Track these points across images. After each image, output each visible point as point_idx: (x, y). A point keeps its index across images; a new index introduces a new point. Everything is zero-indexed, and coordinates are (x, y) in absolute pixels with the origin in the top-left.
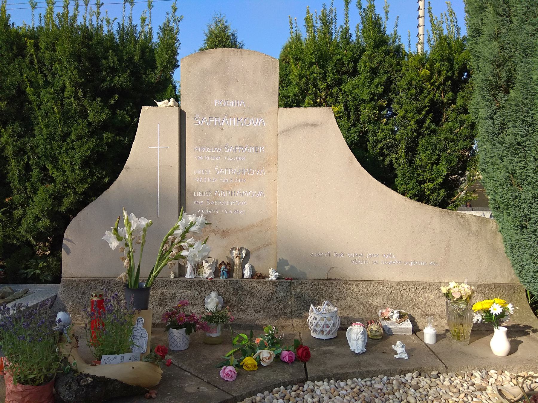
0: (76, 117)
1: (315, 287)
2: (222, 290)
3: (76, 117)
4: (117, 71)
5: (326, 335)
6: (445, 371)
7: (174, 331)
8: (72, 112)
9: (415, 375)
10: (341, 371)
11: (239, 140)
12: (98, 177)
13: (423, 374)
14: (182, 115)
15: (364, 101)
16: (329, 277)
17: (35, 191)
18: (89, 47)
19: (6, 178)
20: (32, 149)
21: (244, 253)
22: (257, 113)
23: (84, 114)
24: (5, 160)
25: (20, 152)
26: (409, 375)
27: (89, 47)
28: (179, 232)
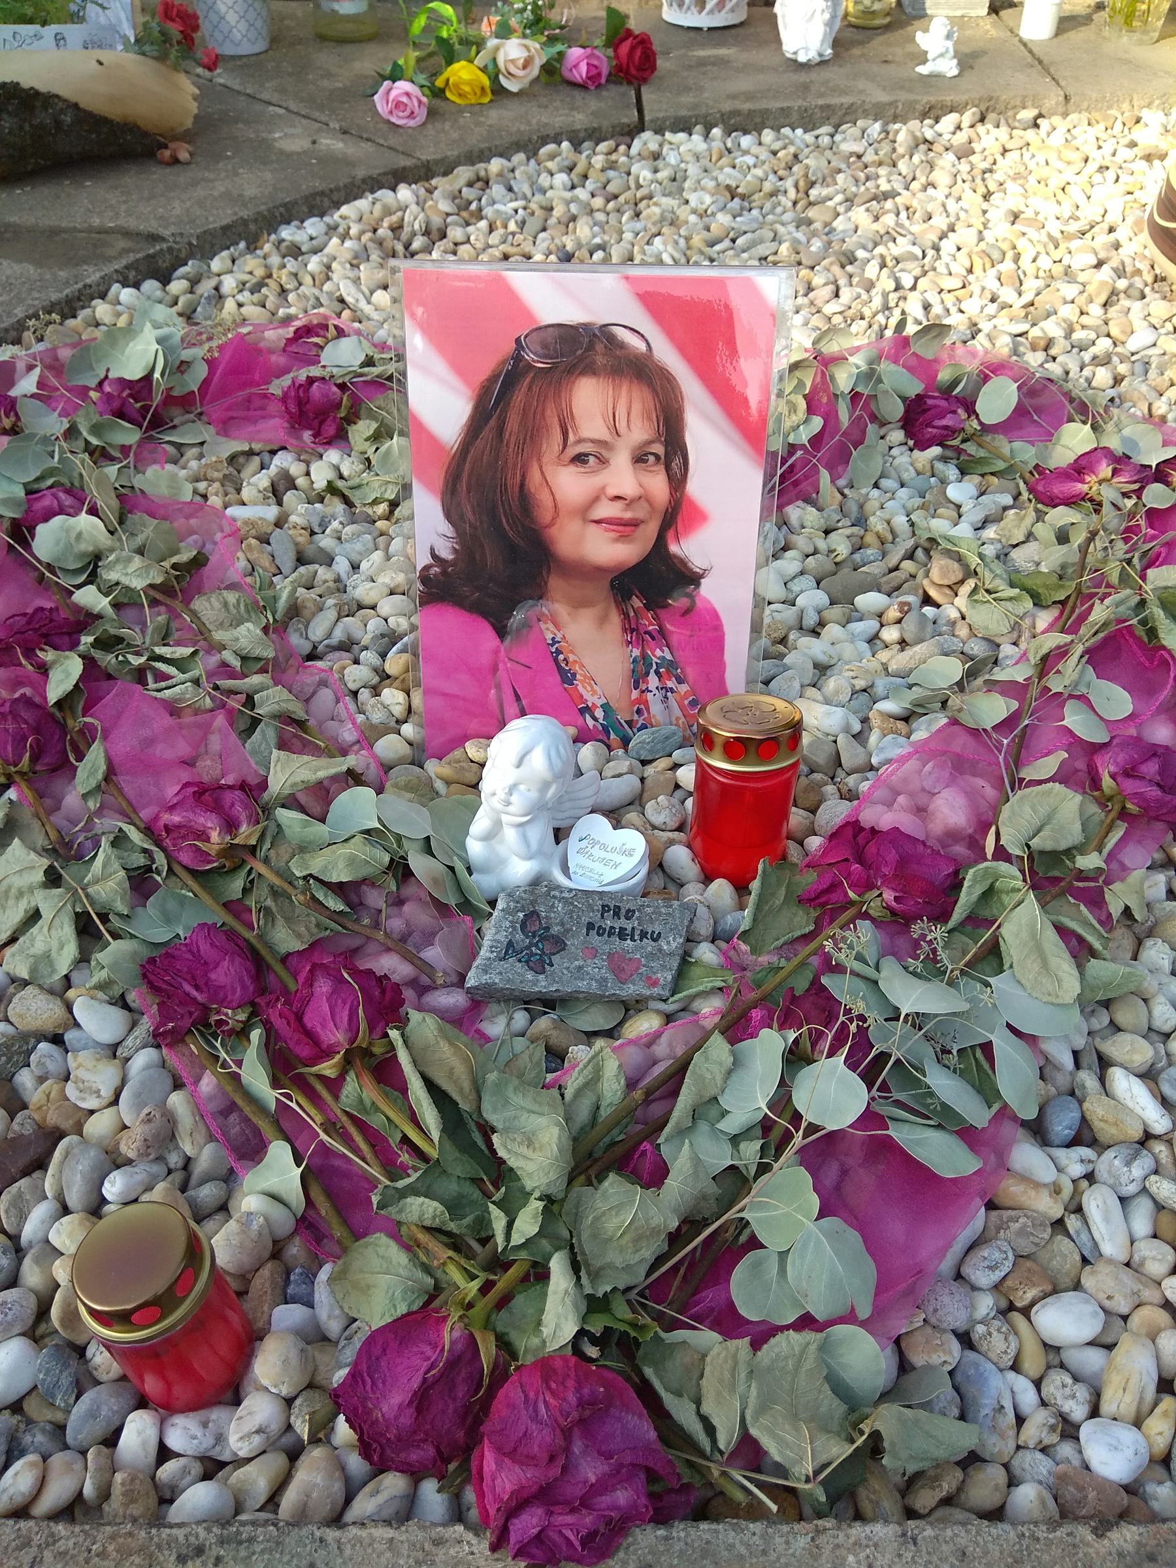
5: (711, 12)
6: (1061, 109)
9: (967, 118)
10: (747, 106)
13: (991, 116)
26: (948, 121)
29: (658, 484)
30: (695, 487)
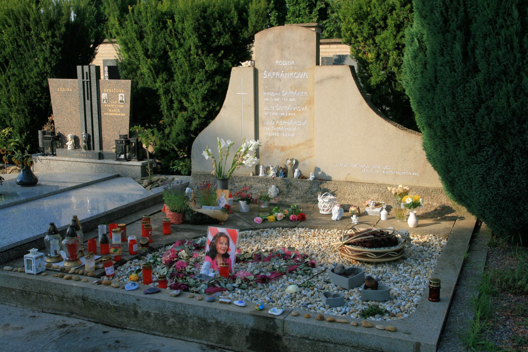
0: (198, 68)
1: (336, 186)
2: (279, 185)
3: (198, 68)
4: (222, 34)
7: (241, 202)
8: (196, 65)
11: (291, 87)
12: (213, 107)
14: (256, 72)
16: (347, 180)
17: (176, 116)
18: (204, 18)
19: (160, 108)
20: (173, 89)
21: (294, 162)
22: (302, 69)
23: (202, 66)
24: (159, 97)
25: (167, 92)
27: (204, 18)
28: (243, 150)
29: (227, 246)
30: (230, 247)
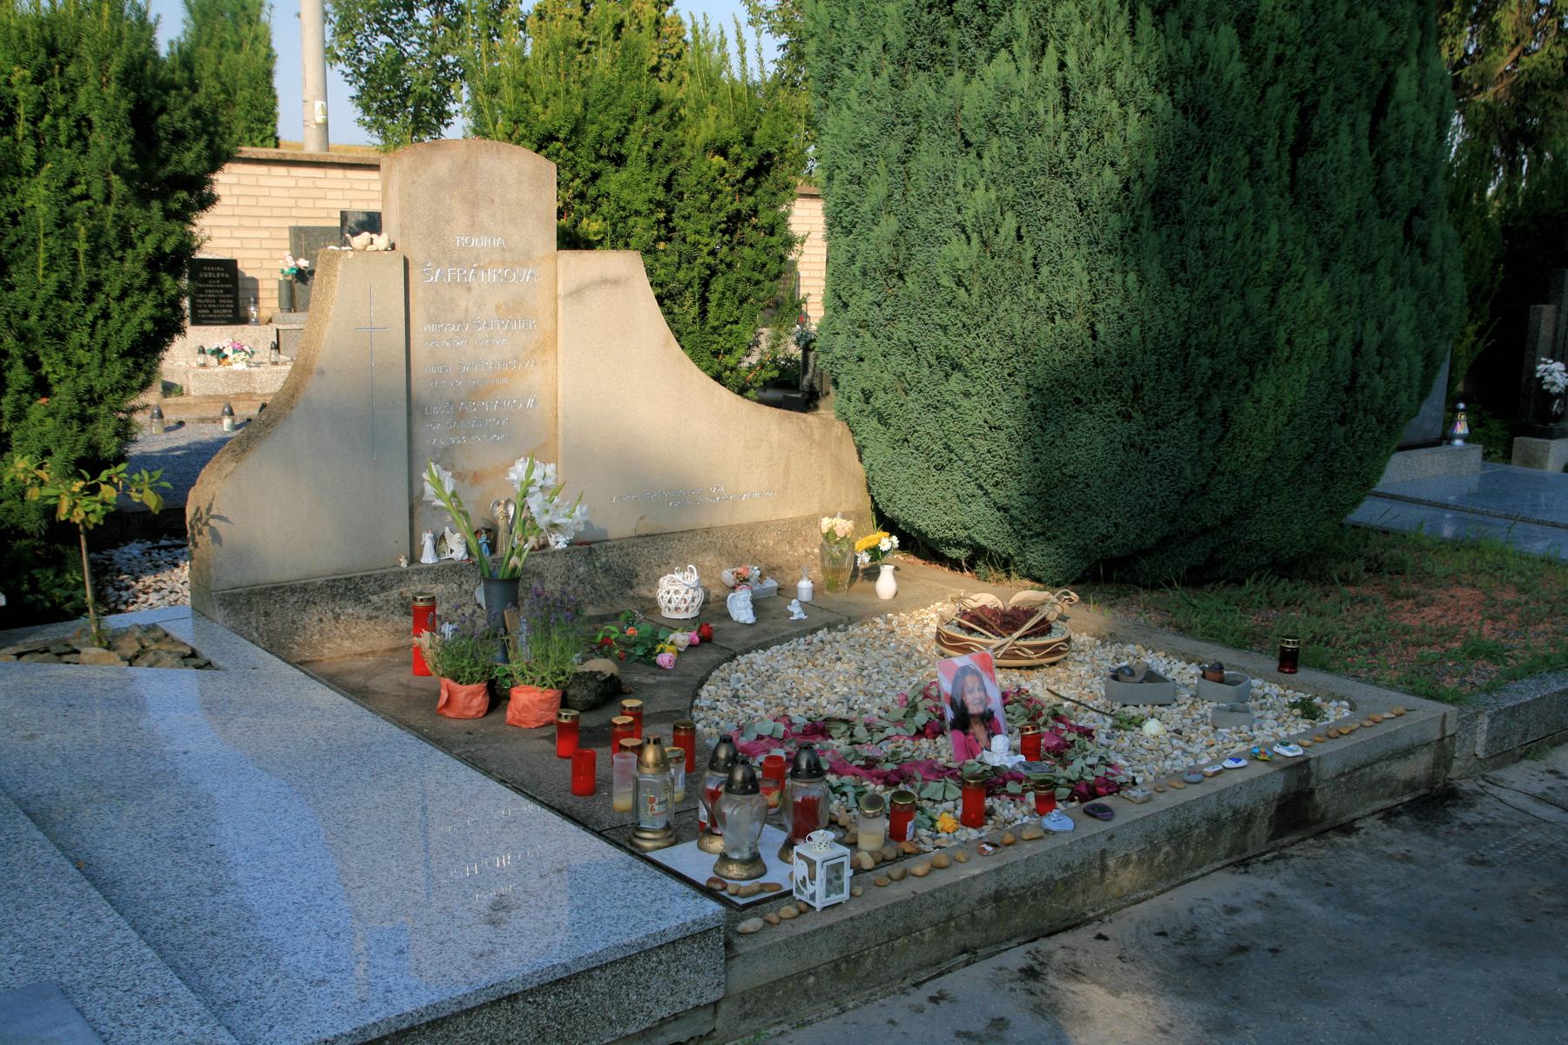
11: (497, 308)
15: (638, 213)
22: (526, 259)
